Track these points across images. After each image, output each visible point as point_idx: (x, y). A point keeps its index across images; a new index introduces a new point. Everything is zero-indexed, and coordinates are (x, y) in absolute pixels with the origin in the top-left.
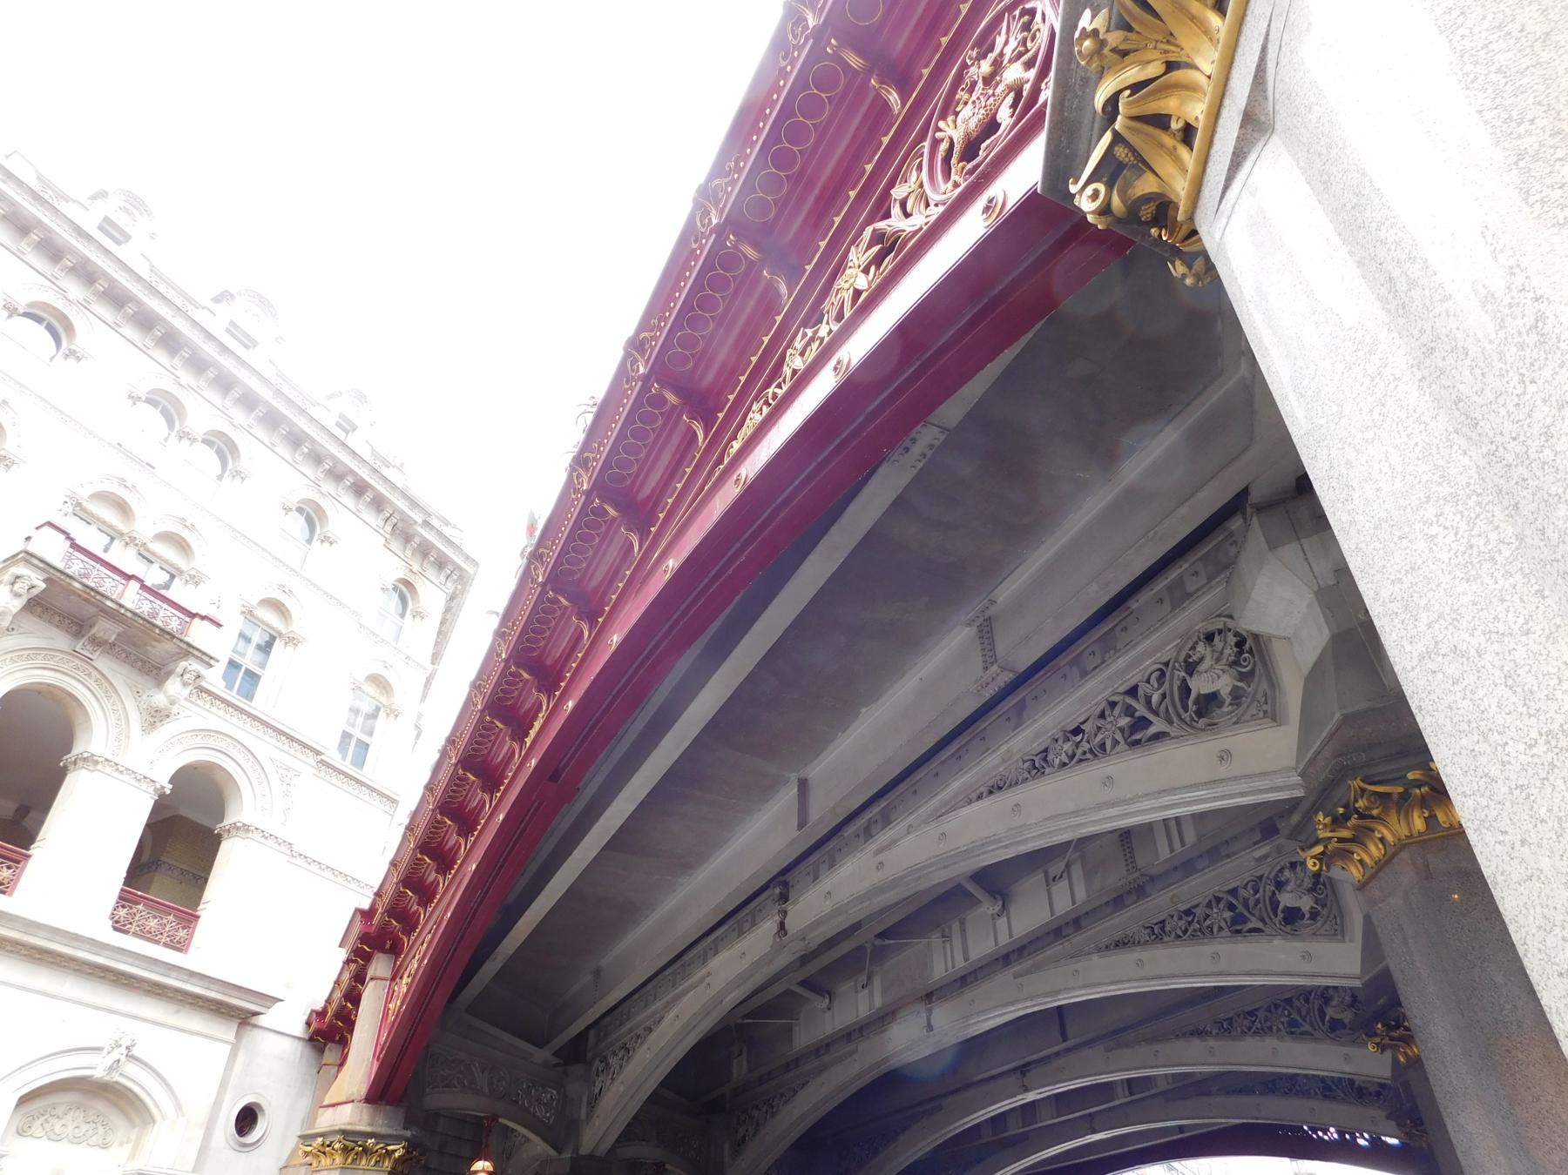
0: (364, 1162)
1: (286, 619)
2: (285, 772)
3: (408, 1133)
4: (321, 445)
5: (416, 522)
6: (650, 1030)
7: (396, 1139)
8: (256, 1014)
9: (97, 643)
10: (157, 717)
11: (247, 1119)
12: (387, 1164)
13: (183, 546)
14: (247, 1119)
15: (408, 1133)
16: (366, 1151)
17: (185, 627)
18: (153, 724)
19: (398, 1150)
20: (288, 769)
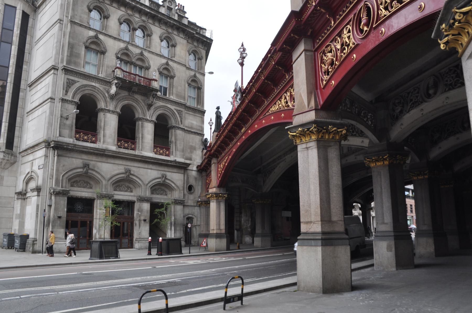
0: (220, 198)
1: (169, 72)
2: (179, 112)
3: (227, 193)
4: (166, 20)
5: (194, 34)
6: (275, 169)
7: (225, 194)
8: (187, 167)
9: (134, 92)
10: (149, 106)
11: (190, 188)
12: (224, 198)
13: (142, 60)
14: (190, 188)
15: (227, 193)
16: (220, 196)
17: (150, 84)
18: (150, 108)
19: (226, 196)
20: (180, 110)
